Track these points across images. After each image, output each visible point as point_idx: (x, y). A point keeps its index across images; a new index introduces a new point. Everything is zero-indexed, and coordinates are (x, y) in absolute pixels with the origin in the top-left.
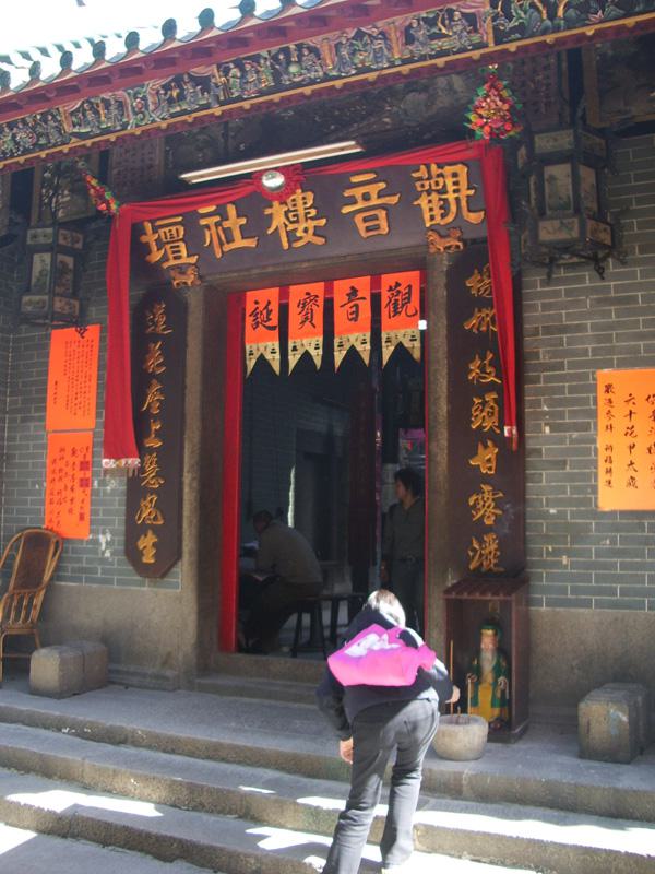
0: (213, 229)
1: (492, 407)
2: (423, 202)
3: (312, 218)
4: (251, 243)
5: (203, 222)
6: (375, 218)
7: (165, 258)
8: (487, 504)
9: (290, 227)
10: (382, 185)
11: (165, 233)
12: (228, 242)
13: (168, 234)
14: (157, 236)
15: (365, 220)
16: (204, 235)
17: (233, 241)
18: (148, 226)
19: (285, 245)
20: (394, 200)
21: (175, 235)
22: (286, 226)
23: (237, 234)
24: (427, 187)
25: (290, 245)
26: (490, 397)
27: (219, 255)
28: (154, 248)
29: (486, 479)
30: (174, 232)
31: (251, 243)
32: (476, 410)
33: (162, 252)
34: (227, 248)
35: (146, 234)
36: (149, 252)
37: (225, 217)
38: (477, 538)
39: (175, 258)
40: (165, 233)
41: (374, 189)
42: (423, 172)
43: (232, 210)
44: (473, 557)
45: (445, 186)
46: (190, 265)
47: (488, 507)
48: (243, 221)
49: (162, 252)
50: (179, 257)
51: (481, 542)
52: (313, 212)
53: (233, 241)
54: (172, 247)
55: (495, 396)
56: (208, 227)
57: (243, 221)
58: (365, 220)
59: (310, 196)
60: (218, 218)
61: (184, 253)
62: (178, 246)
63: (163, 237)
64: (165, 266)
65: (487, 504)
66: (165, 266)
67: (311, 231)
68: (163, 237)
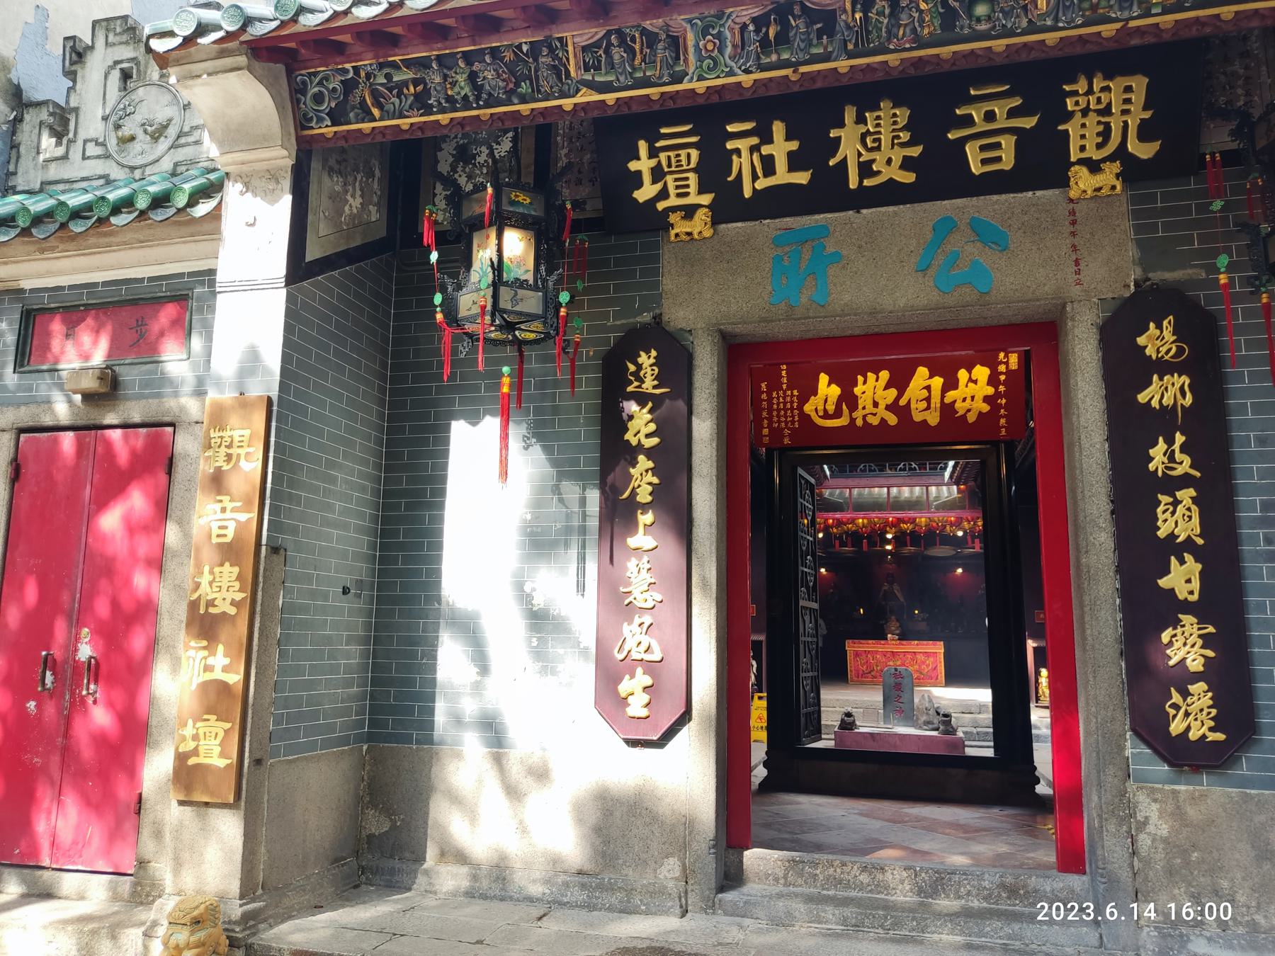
0: (745, 154)
1: (1189, 509)
2: (1072, 128)
3: (903, 145)
4: (802, 178)
5: (730, 145)
6: (997, 146)
7: (664, 194)
8: (1190, 642)
9: (866, 156)
10: (1016, 102)
11: (669, 157)
12: (765, 176)
13: (673, 160)
14: (653, 162)
15: (983, 148)
16: (731, 161)
17: (774, 173)
18: (643, 146)
19: (853, 183)
20: (1029, 123)
21: (684, 162)
22: (860, 155)
23: (781, 164)
24: (1083, 105)
25: (861, 182)
26: (1186, 495)
27: (747, 193)
28: (647, 178)
29: (1187, 607)
30: (683, 158)
31: (802, 178)
32: (1164, 512)
33: (659, 186)
34: (762, 184)
35: (639, 159)
36: (639, 185)
37: (767, 139)
38: (1178, 691)
39: (679, 195)
40: (669, 157)
41: (1000, 108)
42: (1081, 86)
43: (778, 128)
44: (1175, 716)
45: (1109, 104)
46: (700, 206)
47: (1193, 646)
48: (794, 145)
49: (659, 186)
50: (687, 194)
51: (1185, 694)
52: (905, 136)
53: (774, 173)
54: (676, 180)
55: (1194, 494)
56: (738, 152)
57: (794, 145)
58: (983, 148)
59: (903, 115)
60: (754, 140)
61: (693, 188)
62: (687, 179)
63: (664, 163)
64: (661, 206)
65: (1190, 642)
66: (661, 206)
67: (897, 161)
68: (664, 163)
